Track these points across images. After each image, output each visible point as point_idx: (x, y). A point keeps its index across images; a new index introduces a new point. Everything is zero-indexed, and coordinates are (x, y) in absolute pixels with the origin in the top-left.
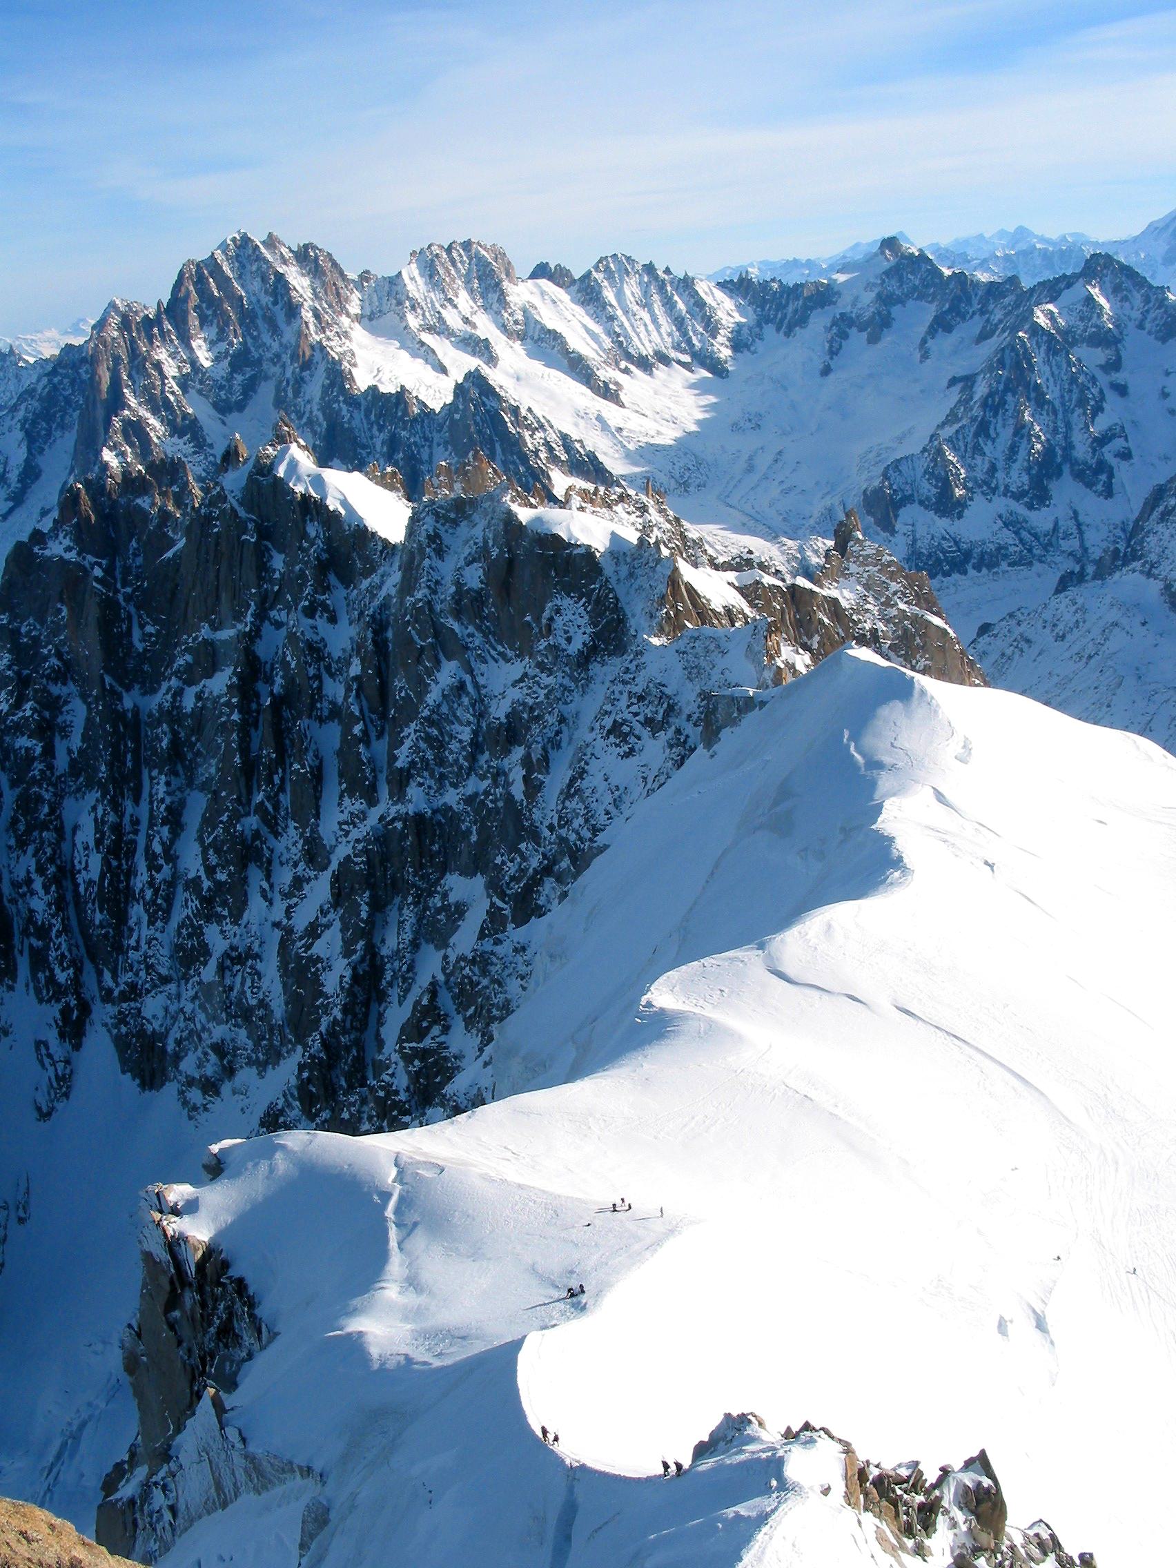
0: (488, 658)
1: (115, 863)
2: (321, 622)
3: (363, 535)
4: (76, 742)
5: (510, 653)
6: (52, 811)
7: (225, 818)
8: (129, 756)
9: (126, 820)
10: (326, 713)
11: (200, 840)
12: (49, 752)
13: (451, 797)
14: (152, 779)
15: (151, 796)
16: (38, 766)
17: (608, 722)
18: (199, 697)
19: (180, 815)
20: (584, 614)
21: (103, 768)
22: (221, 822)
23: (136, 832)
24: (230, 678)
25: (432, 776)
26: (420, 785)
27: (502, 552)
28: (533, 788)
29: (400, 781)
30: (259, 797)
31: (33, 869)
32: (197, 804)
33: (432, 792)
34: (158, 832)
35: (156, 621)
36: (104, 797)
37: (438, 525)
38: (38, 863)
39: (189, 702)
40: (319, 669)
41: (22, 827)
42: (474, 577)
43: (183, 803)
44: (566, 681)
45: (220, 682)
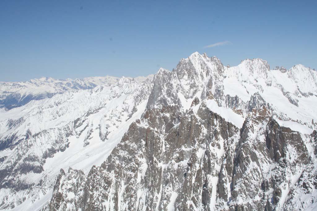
0: (265, 162)
1: (150, 209)
2: (216, 148)
3: (230, 125)
4: (144, 174)
5: (271, 161)
6: (135, 193)
7: (182, 200)
8: (158, 180)
9: (155, 198)
10: (215, 174)
11: (175, 206)
12: (136, 176)
13: (250, 201)
14: (163, 187)
15: (162, 191)
16: (133, 180)
17: (301, 183)
18: (179, 166)
19: (170, 198)
20: (295, 151)
21: (150, 182)
22: (182, 201)
23: (157, 201)
24: (189, 161)
25: (245, 194)
26: (242, 196)
27: (271, 132)
28: (275, 201)
29: (234, 195)
30: (192, 195)
31: (127, 208)
32: (174, 195)
33: (244, 199)
34: (163, 202)
35: (170, 144)
36: (149, 190)
37: (253, 124)
38: (129, 206)
39: (176, 167)
40: (214, 161)
41: (125, 196)
42: (262, 139)
43: (171, 195)
44: (289, 170)
45: (184, 163)
